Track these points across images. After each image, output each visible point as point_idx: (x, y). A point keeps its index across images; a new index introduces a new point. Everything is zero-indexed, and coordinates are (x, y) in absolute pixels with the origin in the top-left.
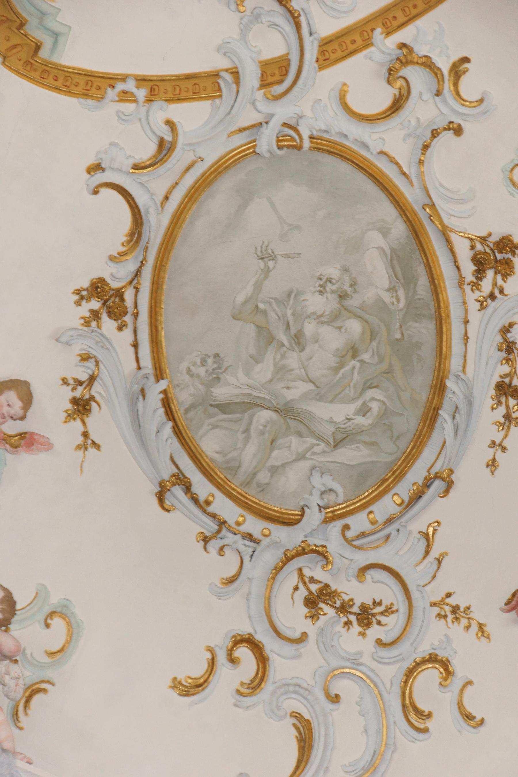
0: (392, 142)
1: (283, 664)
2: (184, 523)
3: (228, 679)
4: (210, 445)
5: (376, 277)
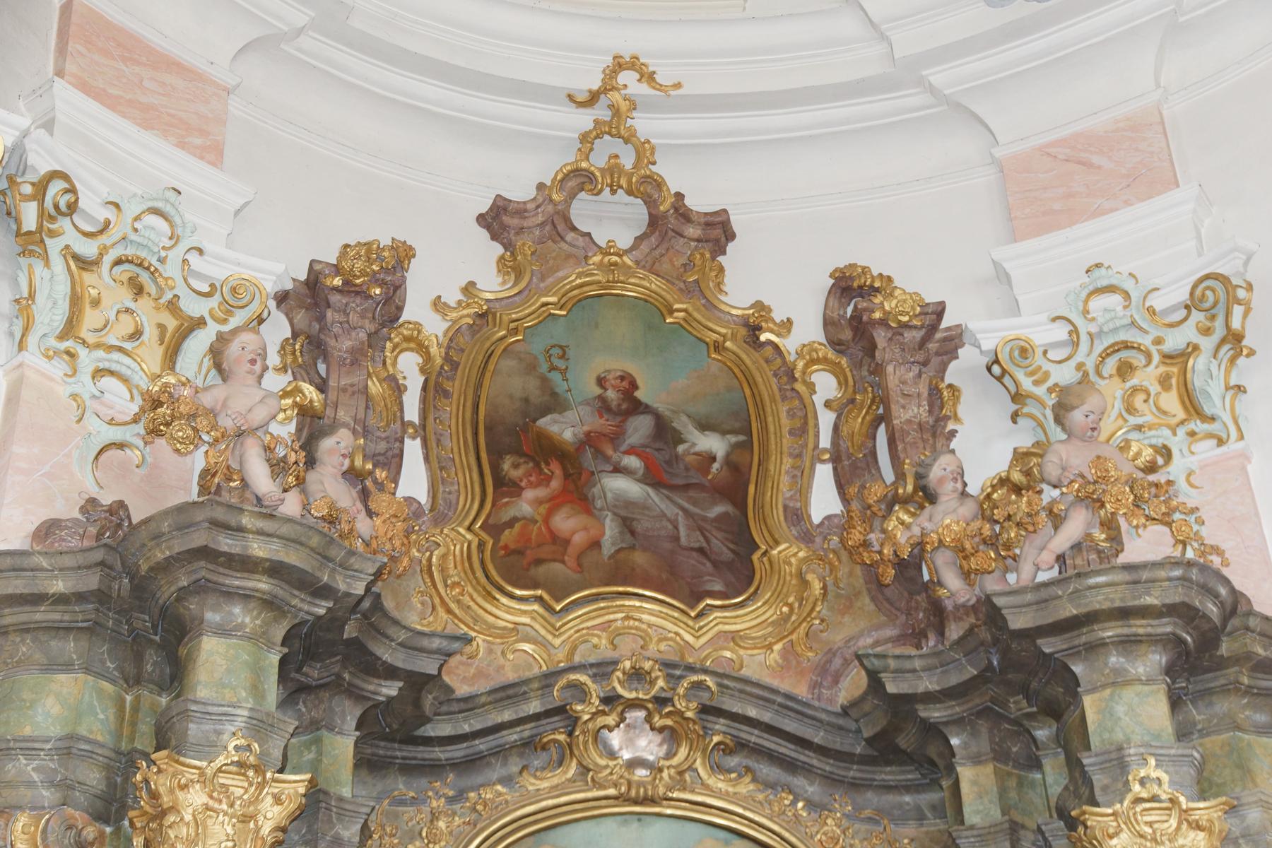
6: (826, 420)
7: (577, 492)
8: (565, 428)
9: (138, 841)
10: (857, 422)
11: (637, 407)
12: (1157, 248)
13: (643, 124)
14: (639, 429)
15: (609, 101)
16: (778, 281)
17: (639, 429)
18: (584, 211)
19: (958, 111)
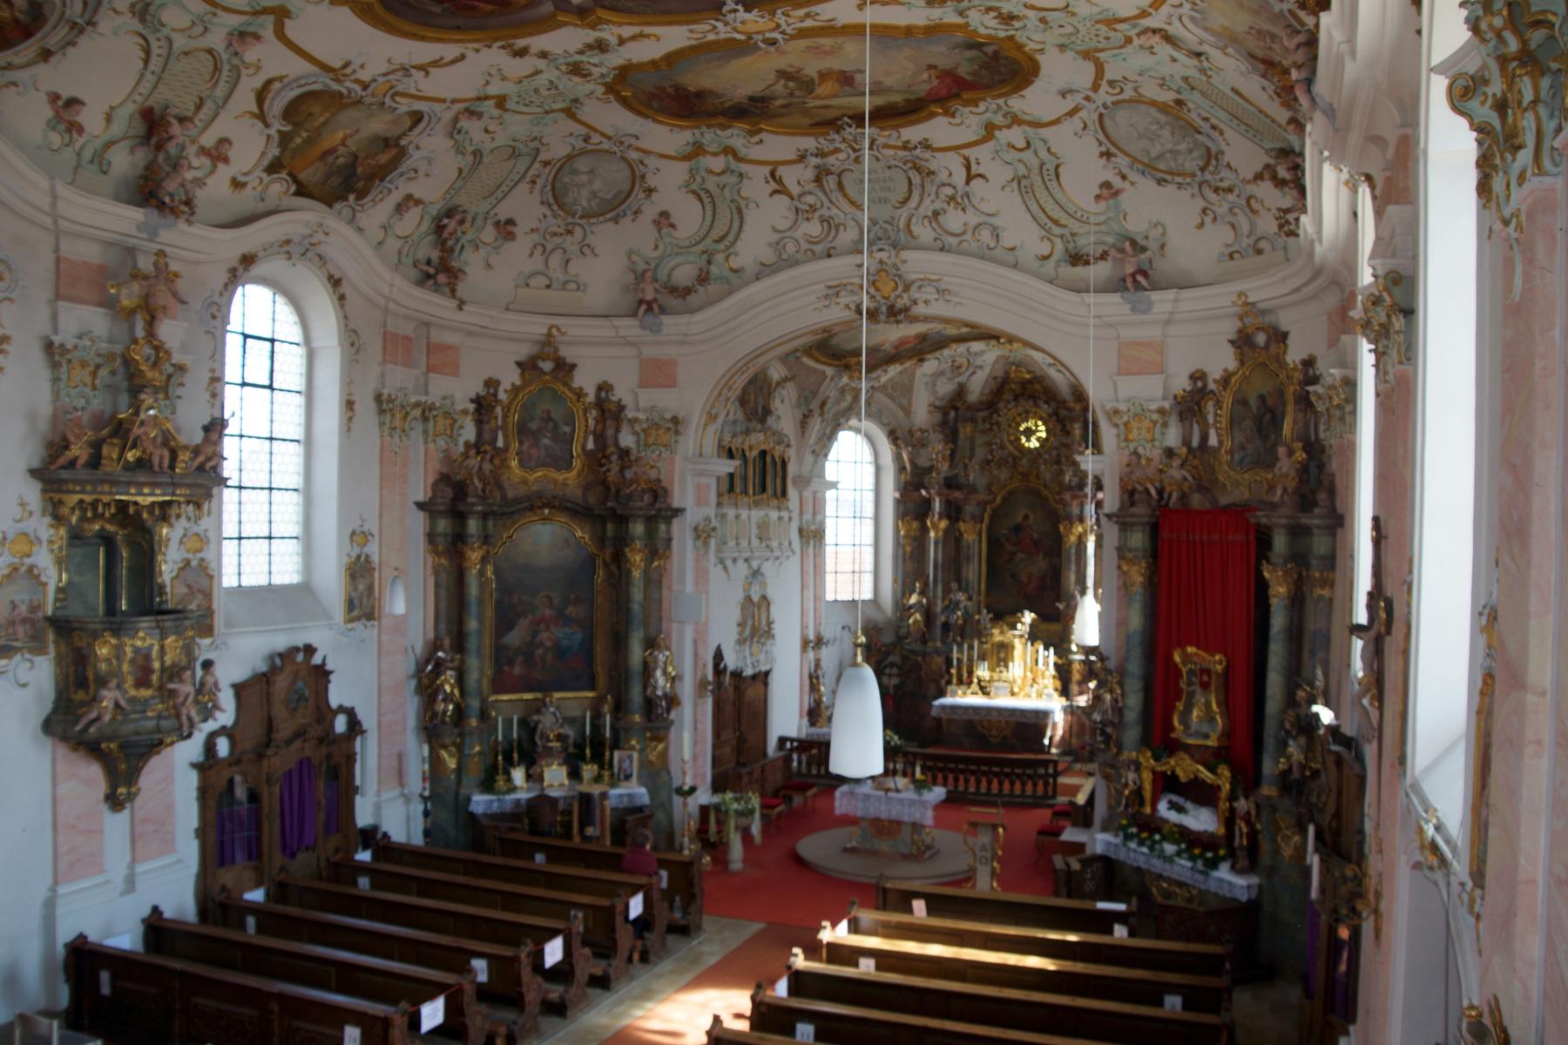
0: (1127, 95)
1: (1220, 211)
2: (1171, 188)
3: (1208, 219)
4: (1162, 166)
5: (1162, 118)
7: (536, 444)
8: (534, 426)
10: (600, 427)
11: (550, 419)
13: (559, 338)
14: (551, 425)
15: (548, 342)
16: (586, 380)
17: (551, 425)
18: (541, 364)
19: (633, 344)
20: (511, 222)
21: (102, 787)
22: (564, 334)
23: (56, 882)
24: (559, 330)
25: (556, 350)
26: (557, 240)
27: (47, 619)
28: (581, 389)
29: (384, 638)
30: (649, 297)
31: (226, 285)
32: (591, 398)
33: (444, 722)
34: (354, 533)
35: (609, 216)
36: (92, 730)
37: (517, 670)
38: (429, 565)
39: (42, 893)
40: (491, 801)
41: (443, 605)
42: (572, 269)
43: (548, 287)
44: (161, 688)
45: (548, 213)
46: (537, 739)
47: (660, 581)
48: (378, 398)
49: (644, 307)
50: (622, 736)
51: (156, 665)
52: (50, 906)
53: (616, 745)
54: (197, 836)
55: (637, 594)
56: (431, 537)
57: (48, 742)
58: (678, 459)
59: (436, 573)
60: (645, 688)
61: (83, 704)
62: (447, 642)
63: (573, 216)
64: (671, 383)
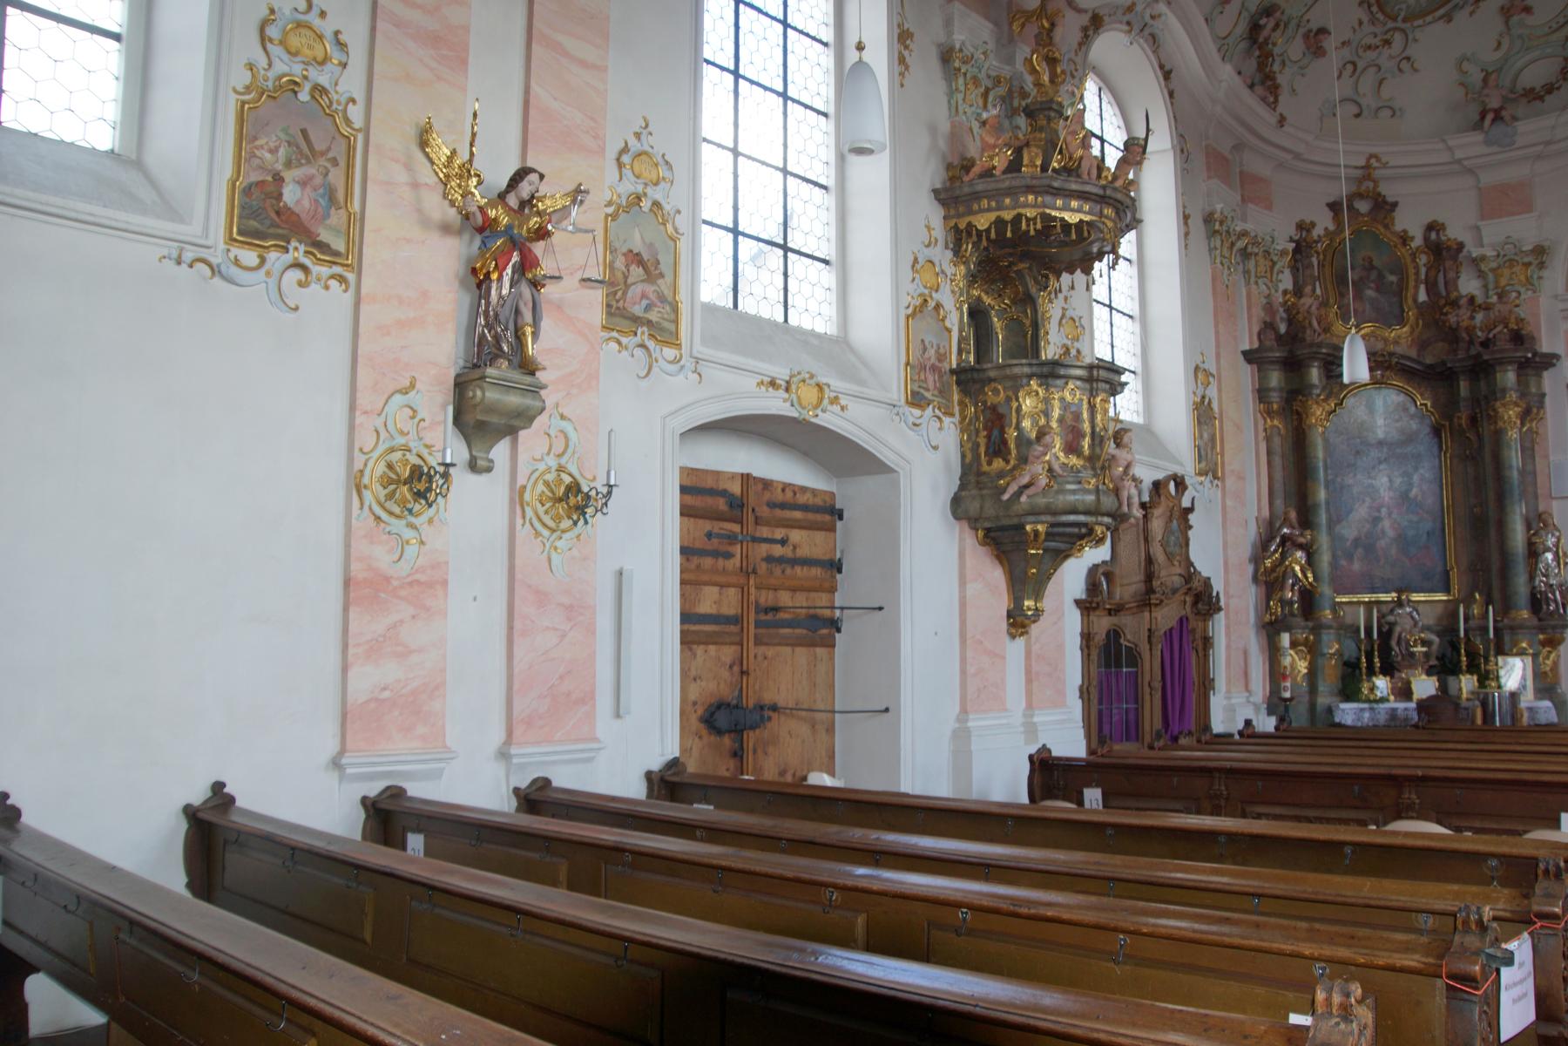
6: (1423, 270)
9: (788, 198)
10: (1433, 273)
11: (1372, 267)
12: (1524, 230)
13: (1378, 174)
14: (1374, 275)
16: (1411, 221)
17: (1374, 275)
19: (1470, 171)
20: (1323, 31)
21: (1003, 603)
22: (1385, 166)
23: (964, 710)
24: (1378, 160)
25: (1375, 182)
26: (1371, 55)
27: (952, 372)
28: (1405, 231)
29: (1229, 503)
30: (1494, 103)
31: (1080, 45)
32: (1418, 242)
33: (1292, 615)
34: (1197, 368)
35: (1442, 11)
36: (1023, 499)
37: (1356, 566)
38: (1261, 428)
39: (951, 724)
40: (1362, 710)
41: (1278, 475)
42: (1386, 92)
43: (1358, 116)
44: (1092, 459)
45: (1365, 19)
46: (1393, 643)
47: (1533, 449)
48: (1208, 219)
49: (1490, 117)
50: (1507, 639)
51: (1086, 427)
52: (961, 736)
53: (1501, 651)
54: (1081, 697)
55: (1514, 458)
56: (1262, 394)
57: (957, 526)
58: (1544, 302)
59: (1268, 439)
60: (1532, 578)
61: (1001, 474)
62: (1293, 515)
63: (1395, 19)
64: (1526, 206)
